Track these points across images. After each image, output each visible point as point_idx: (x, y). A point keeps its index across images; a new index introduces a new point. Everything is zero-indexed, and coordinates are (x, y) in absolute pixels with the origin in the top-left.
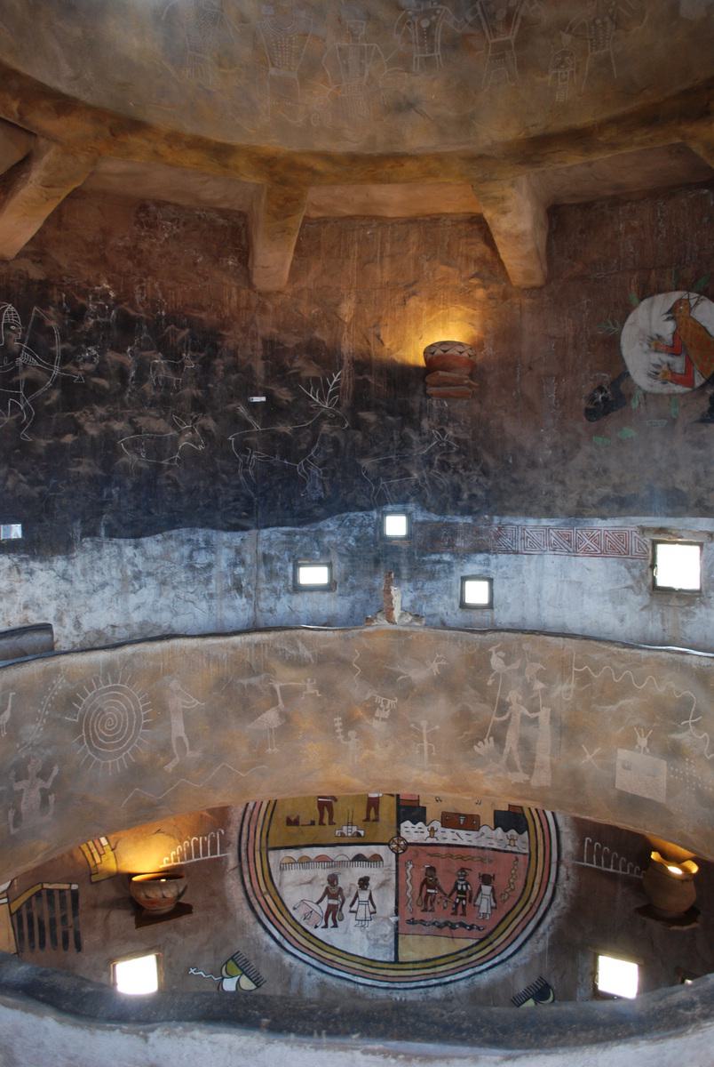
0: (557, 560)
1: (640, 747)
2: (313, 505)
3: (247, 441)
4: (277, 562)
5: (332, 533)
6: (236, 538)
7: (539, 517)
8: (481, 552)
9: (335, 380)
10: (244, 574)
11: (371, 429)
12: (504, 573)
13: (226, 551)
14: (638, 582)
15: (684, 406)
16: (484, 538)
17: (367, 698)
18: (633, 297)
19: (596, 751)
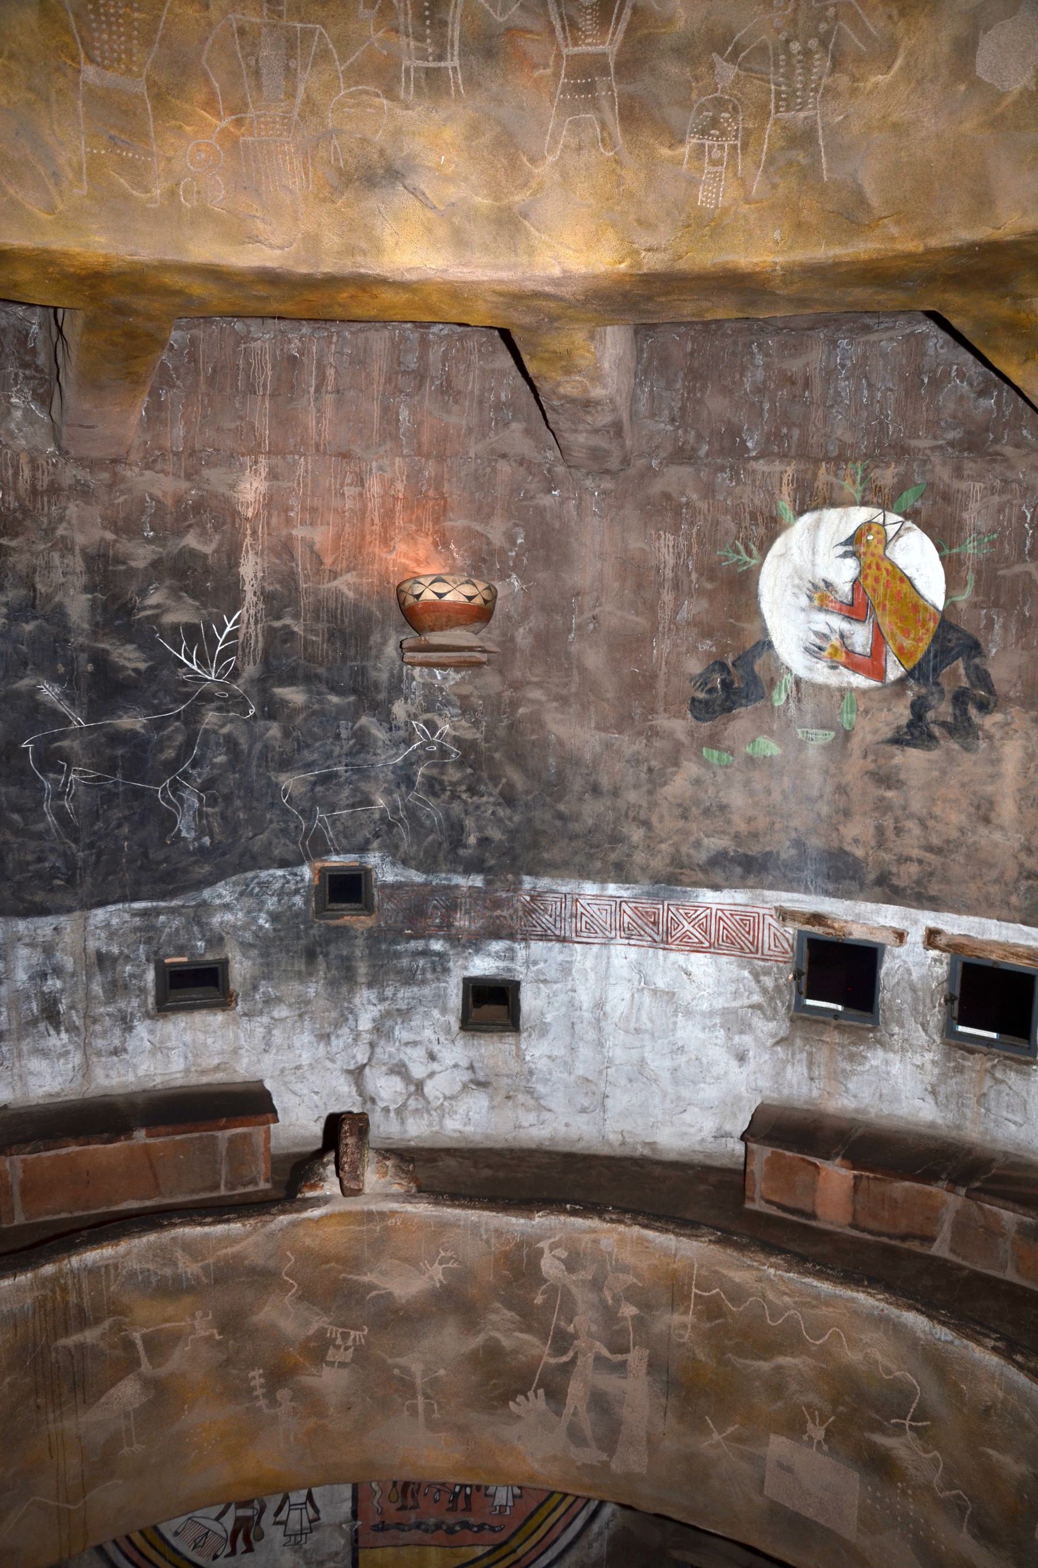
0: (633, 953)
1: (811, 1438)
2: (192, 859)
3: (60, 747)
4: (126, 963)
5: (227, 907)
6: (44, 926)
7: (604, 881)
8: (497, 936)
9: (228, 629)
10: (62, 990)
11: (299, 720)
12: (540, 972)
13: (23, 952)
14: (772, 998)
15: (866, 712)
16: (505, 913)
17: (311, 1332)
18: (785, 505)
19: (730, 1430)
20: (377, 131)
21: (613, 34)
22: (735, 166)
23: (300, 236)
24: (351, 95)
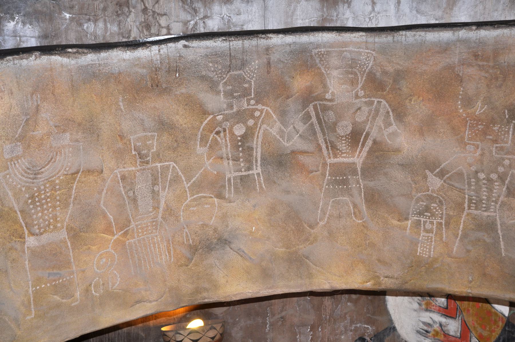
20: (211, 218)
21: (360, 153)
22: (441, 234)
23: (167, 289)
24: (195, 200)
